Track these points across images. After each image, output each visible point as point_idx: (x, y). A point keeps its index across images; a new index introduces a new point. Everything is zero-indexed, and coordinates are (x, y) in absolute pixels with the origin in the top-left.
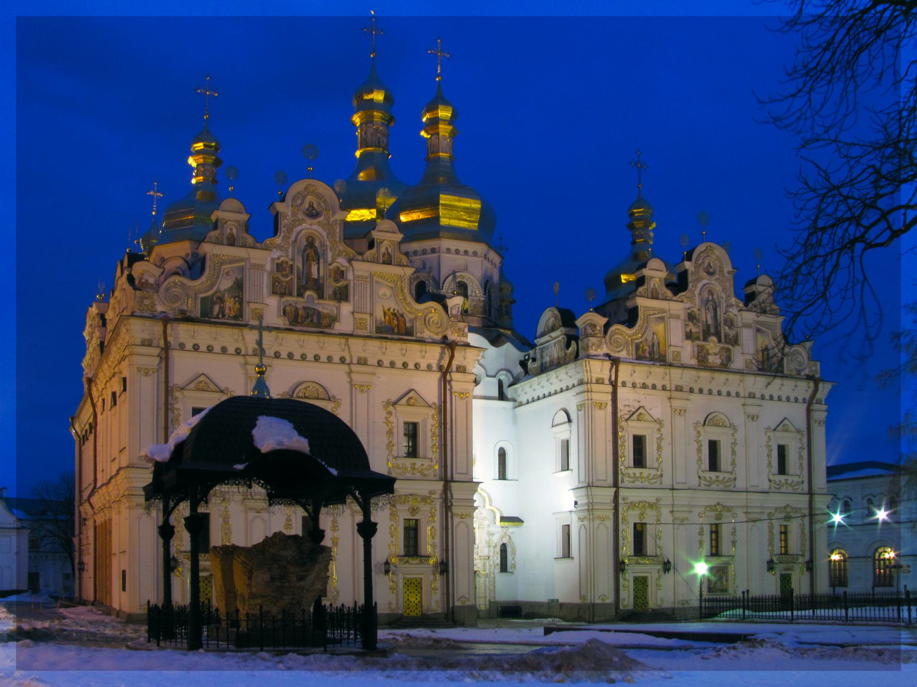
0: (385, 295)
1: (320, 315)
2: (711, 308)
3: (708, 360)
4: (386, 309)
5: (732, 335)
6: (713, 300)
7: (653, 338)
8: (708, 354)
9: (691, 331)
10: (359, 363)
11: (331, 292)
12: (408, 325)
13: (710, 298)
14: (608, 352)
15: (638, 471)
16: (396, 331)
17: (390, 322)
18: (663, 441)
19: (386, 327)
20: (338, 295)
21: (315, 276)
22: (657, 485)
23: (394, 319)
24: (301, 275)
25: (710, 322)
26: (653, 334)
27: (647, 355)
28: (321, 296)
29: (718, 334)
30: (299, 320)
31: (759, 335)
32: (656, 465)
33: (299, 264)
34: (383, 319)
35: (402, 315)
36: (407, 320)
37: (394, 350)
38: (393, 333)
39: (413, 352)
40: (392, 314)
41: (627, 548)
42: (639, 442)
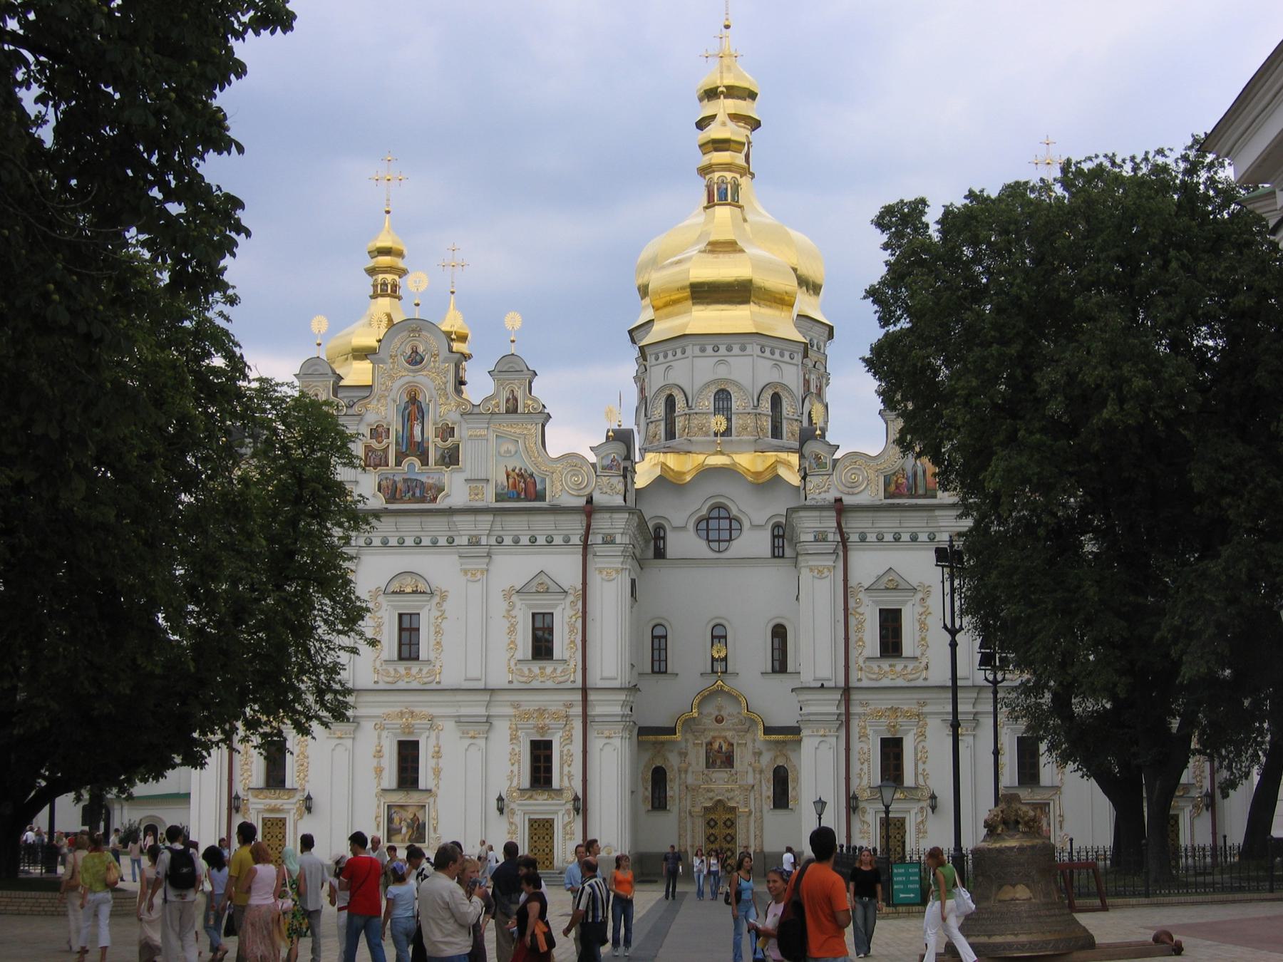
0: (508, 451)
1: (424, 487)
4: (510, 469)
10: (470, 544)
11: (437, 458)
12: (539, 487)
14: (838, 495)
15: (885, 665)
16: (523, 497)
17: (515, 486)
18: (929, 617)
19: (507, 494)
20: (447, 459)
21: (418, 438)
22: (920, 683)
23: (519, 482)
24: (400, 440)
28: (425, 462)
30: (397, 496)
32: (918, 654)
33: (396, 426)
34: (506, 484)
35: (531, 475)
37: (517, 525)
38: (518, 499)
39: (543, 526)
40: (518, 475)
41: (869, 771)
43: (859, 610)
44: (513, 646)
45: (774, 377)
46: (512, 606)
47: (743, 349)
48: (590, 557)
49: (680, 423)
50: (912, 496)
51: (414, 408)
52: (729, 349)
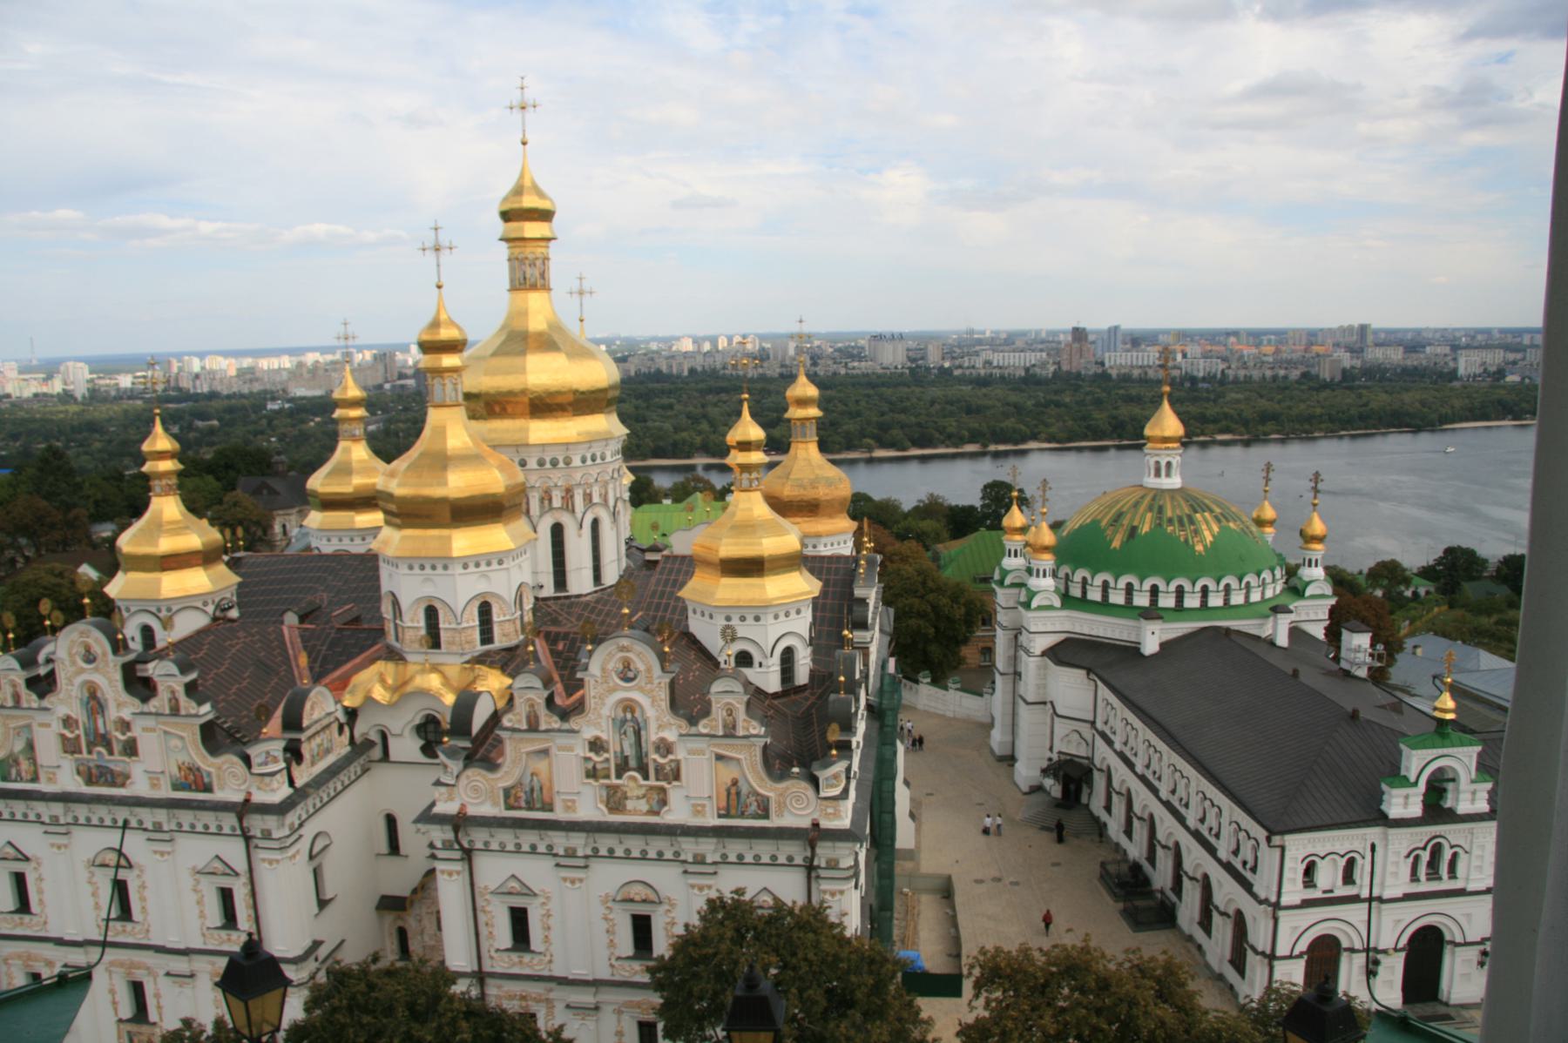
2: (630, 731)
3: (625, 806)
5: (668, 768)
6: (634, 719)
7: (532, 780)
8: (626, 798)
9: (594, 768)
12: (206, 780)
13: (629, 716)
17: (186, 778)
21: (102, 731)
25: (629, 751)
26: (532, 774)
27: (523, 804)
28: (111, 753)
29: (643, 770)
31: (721, 765)
35: (198, 769)
36: (205, 775)
39: (209, 818)
42: (519, 919)
43: (488, 909)
44: (202, 915)
45: (482, 587)
46: (198, 882)
47: (445, 567)
48: (252, 850)
49: (400, 630)
50: (530, 808)
51: (95, 705)
52: (434, 568)
